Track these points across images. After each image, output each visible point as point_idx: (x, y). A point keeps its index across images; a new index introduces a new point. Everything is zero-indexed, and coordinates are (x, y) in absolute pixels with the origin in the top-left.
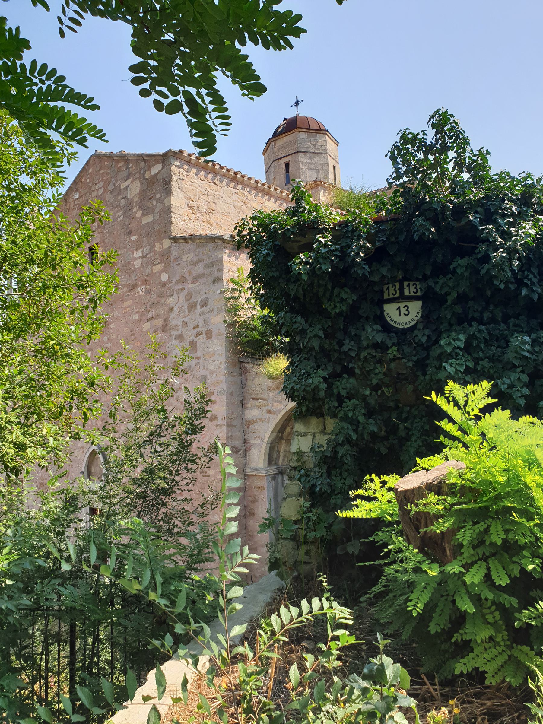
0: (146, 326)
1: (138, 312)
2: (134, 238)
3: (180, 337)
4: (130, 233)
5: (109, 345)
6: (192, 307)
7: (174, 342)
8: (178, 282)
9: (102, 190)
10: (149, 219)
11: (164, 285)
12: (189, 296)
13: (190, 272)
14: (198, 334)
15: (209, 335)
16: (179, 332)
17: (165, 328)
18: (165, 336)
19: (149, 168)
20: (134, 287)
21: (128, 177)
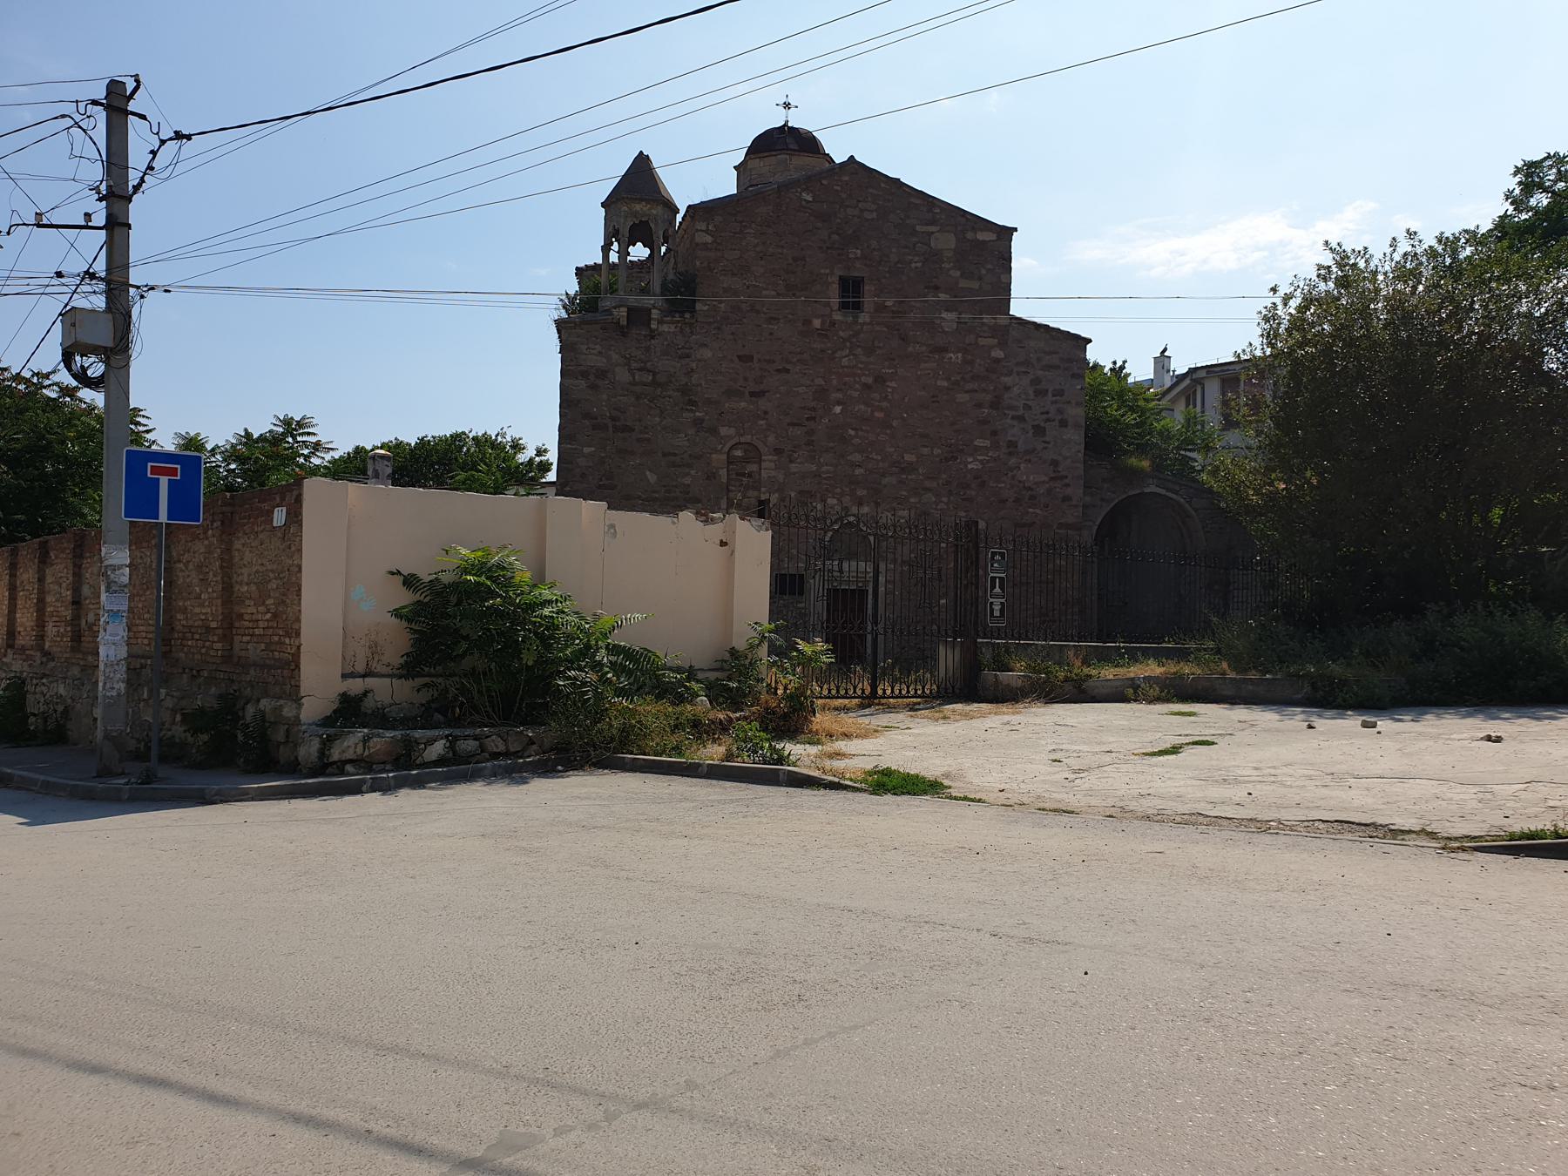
0: (962, 397)
1: (948, 379)
2: (943, 296)
3: (1021, 419)
4: (937, 288)
5: (885, 404)
6: (1040, 393)
7: (1009, 421)
8: (1017, 364)
9: (875, 215)
10: (975, 285)
11: (997, 361)
12: (1036, 381)
13: (1039, 360)
14: (1048, 420)
15: (1063, 423)
16: (1020, 412)
17: (995, 404)
18: (994, 413)
19: (974, 229)
20: (943, 350)
21: (932, 222)
